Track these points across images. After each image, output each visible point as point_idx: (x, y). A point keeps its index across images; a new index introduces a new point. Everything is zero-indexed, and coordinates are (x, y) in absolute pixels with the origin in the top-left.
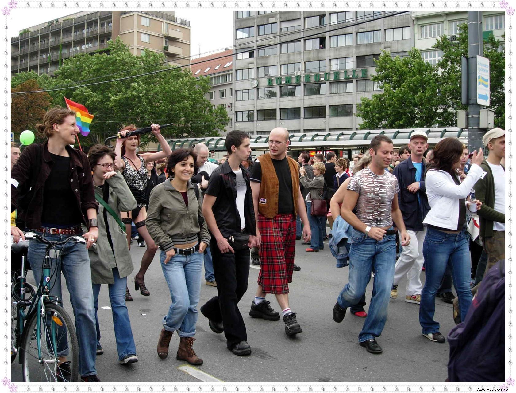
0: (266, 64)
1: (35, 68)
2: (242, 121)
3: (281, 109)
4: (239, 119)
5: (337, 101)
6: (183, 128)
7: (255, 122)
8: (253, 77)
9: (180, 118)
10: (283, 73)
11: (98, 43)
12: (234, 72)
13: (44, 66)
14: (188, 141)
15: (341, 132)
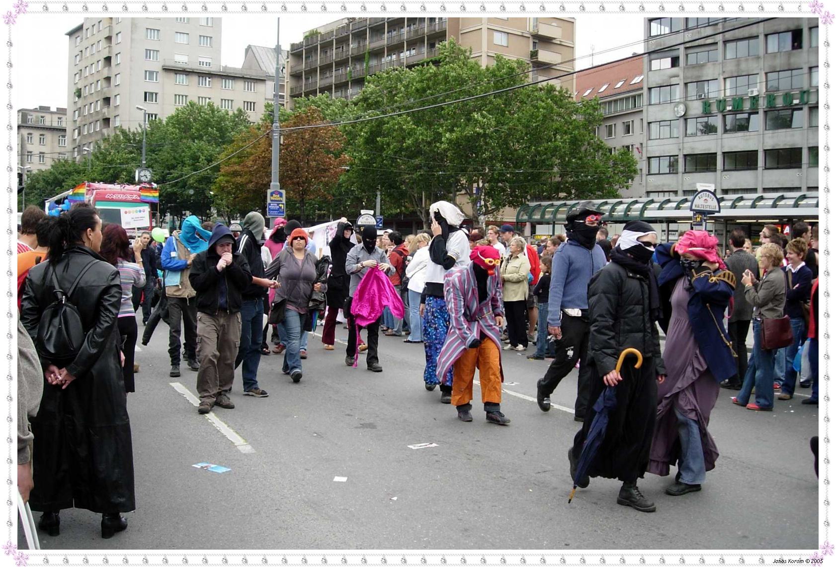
0: (699, 77)
1: (328, 88)
4: (654, 170)
6: (559, 183)
7: (680, 175)
10: (728, 94)
13: (342, 86)
14: (565, 205)
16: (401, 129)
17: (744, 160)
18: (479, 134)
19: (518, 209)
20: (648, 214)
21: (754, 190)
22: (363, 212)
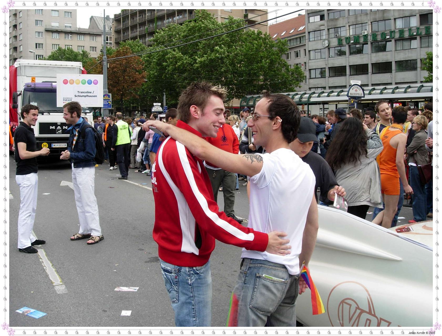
1: (134, 38)
2: (315, 78)
3: (350, 66)
4: (313, 76)
5: (402, 56)
6: (262, 85)
7: (327, 78)
8: (324, 37)
9: (259, 76)
10: (351, 34)
12: (307, 34)
13: (142, 36)
15: (408, 85)
16: (176, 57)
17: (360, 70)
18: (218, 58)
19: (241, 99)
20: (312, 100)
21: (391, 84)
22: (155, 104)
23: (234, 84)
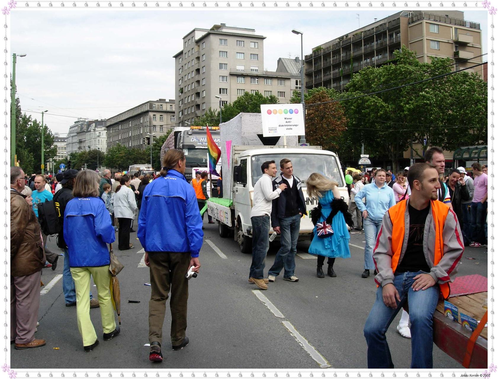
11: (388, 55)
13: (337, 80)
19: (453, 152)
23: (446, 134)
